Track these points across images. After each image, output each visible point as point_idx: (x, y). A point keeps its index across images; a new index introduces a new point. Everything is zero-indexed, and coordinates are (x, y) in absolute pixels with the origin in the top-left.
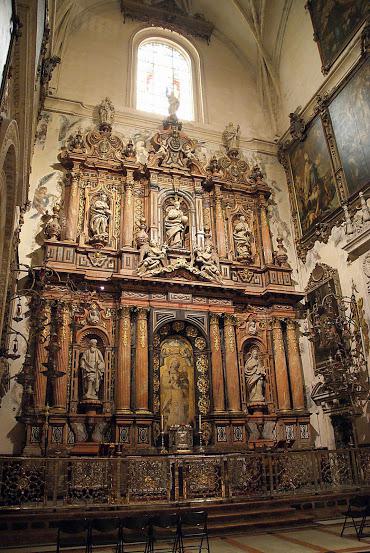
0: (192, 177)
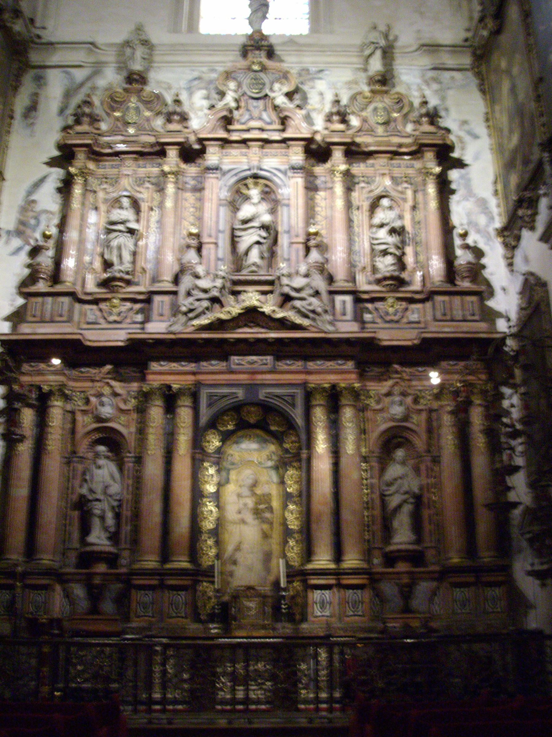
0: (284, 141)
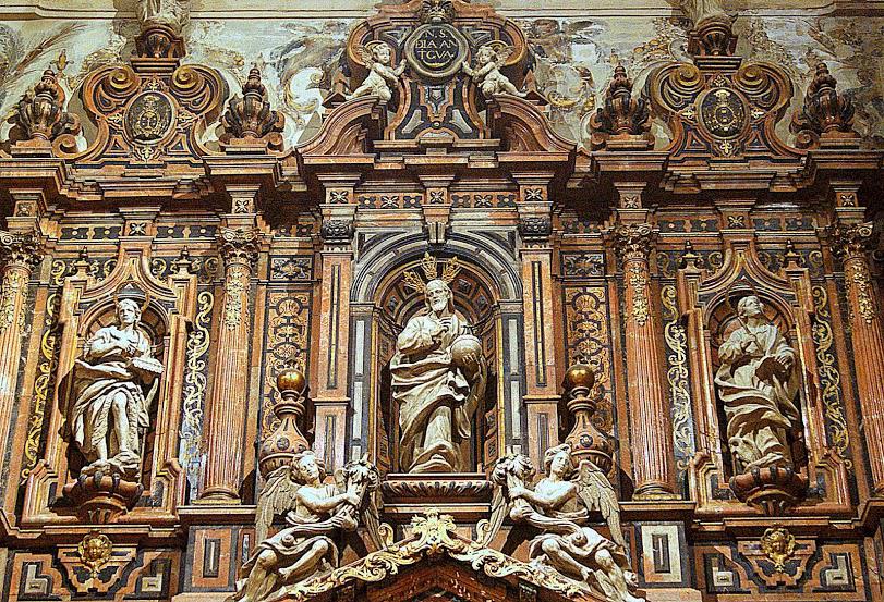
0: (504, 170)
